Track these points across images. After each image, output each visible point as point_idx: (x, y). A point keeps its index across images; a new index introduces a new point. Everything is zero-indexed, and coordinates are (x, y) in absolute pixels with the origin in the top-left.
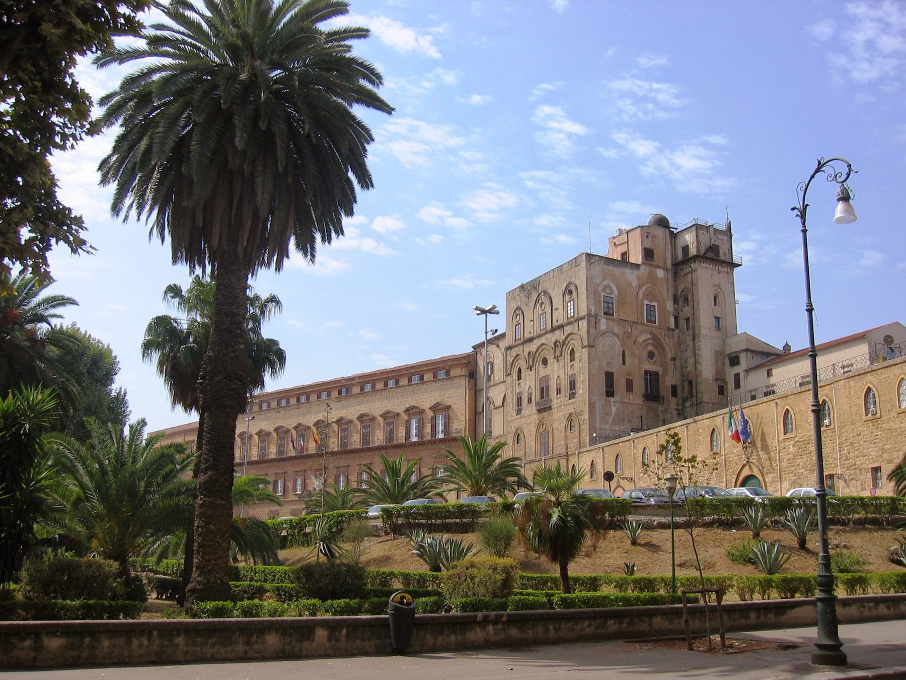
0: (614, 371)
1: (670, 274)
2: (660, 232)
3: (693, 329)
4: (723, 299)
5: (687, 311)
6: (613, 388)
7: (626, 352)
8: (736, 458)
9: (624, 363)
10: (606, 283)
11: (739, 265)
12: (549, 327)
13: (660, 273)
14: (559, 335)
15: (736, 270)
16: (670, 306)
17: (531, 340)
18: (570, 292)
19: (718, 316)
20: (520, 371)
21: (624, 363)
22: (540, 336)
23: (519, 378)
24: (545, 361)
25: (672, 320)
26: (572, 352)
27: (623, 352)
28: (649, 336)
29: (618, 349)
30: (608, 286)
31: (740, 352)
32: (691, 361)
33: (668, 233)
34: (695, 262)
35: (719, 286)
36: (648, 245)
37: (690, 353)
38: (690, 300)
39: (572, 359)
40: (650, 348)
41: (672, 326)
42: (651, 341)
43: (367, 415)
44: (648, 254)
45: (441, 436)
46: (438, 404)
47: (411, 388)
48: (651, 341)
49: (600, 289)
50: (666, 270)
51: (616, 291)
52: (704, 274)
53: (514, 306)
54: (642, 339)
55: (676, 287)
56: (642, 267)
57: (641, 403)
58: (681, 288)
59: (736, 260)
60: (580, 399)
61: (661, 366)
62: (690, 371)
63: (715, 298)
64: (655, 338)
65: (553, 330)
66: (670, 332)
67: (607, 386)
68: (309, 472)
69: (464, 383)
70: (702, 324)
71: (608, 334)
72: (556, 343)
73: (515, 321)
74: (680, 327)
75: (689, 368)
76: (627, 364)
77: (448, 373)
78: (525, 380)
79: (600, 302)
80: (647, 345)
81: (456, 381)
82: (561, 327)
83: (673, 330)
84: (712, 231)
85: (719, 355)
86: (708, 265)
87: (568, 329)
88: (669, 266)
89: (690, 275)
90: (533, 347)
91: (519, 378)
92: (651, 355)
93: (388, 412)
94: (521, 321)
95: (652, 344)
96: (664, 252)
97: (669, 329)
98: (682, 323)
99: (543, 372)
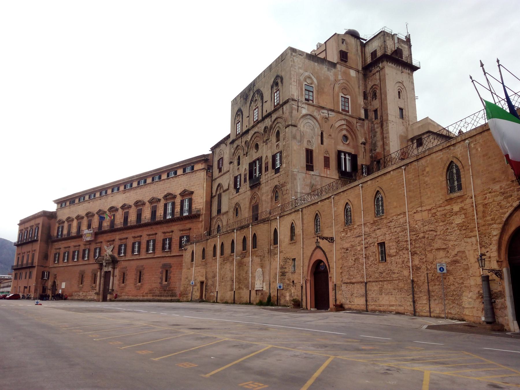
0: (314, 148)
1: (361, 75)
2: (352, 41)
3: (382, 116)
4: (406, 92)
5: (376, 104)
6: (312, 162)
7: (324, 133)
8: (500, 198)
9: (322, 143)
10: (307, 74)
11: (419, 68)
12: (260, 118)
13: (353, 73)
14: (268, 122)
15: (416, 74)
16: (361, 100)
17: (247, 132)
18: (277, 84)
19: (402, 107)
20: (239, 158)
21: (322, 143)
22: (253, 127)
23: (239, 164)
24: (257, 147)
25: (363, 112)
26: (278, 133)
27: (322, 133)
28: (343, 122)
29: (318, 131)
30: (310, 78)
31: (423, 134)
32: (379, 144)
33: (359, 44)
34: (382, 62)
35: (402, 83)
36: (343, 48)
37: (378, 135)
38: (378, 95)
39: (278, 140)
40: (344, 132)
41: (363, 117)
42: (345, 127)
43: (140, 201)
44: (344, 56)
45: (186, 214)
46: (185, 191)
47: (169, 180)
48: (345, 127)
49: (302, 78)
50: (358, 71)
51: (315, 80)
52: (391, 72)
53: (236, 109)
54: (337, 125)
55: (366, 86)
56: (338, 66)
57: (337, 178)
58: (370, 84)
59: (415, 63)
60: (283, 172)
61: (354, 148)
62: (378, 153)
63: (399, 92)
64: (349, 124)
65: (264, 119)
66: (361, 121)
67: (307, 161)
68: (104, 243)
69: (202, 175)
70: (389, 112)
71: (308, 117)
72: (265, 128)
73: (236, 120)
74: (369, 118)
75: (378, 151)
76: (325, 143)
77: (193, 168)
78: (243, 164)
79: (302, 89)
80: (342, 130)
81: (198, 173)
82: (269, 115)
83: (363, 120)
84: (396, 41)
85: (402, 138)
86: (393, 65)
87: (274, 116)
88: (360, 68)
89: (378, 74)
90: (249, 137)
91: (239, 164)
92: (345, 137)
93: (153, 198)
94: (241, 120)
95: (347, 130)
96: (356, 59)
97: (360, 119)
98: (372, 115)
99: (254, 155)
